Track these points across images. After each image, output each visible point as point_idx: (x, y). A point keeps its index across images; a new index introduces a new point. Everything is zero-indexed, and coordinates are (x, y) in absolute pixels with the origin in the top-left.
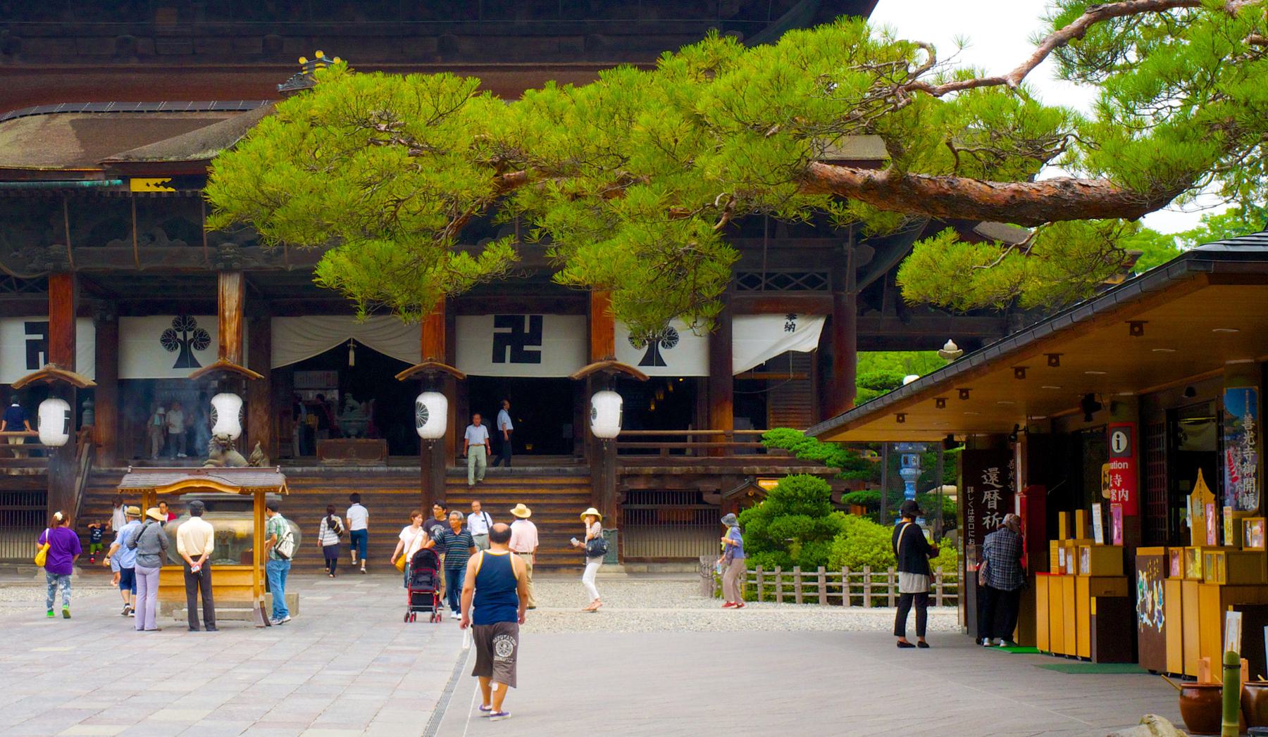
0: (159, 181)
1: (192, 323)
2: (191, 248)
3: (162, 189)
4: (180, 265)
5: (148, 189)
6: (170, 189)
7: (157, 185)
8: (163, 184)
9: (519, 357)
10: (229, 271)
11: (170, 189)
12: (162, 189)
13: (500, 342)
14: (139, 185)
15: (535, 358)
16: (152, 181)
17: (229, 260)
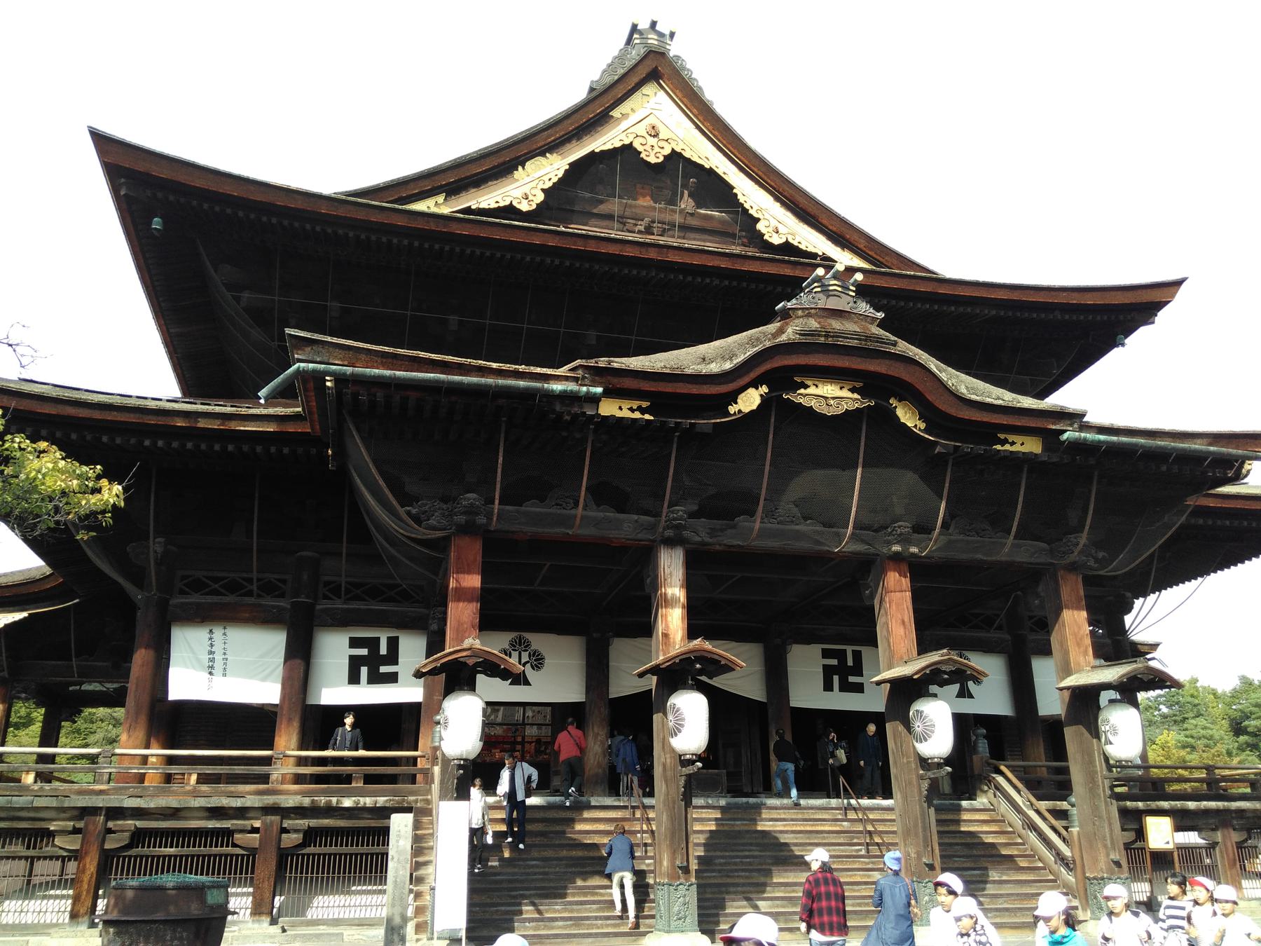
0: (635, 404)
1: (528, 645)
2: (622, 516)
3: (637, 415)
4: (613, 534)
5: (619, 414)
6: (647, 417)
7: (632, 410)
8: (640, 409)
9: (847, 687)
10: (671, 543)
11: (647, 417)
12: (637, 415)
13: (828, 672)
14: (609, 408)
15: (859, 688)
16: (626, 404)
17: (678, 527)
